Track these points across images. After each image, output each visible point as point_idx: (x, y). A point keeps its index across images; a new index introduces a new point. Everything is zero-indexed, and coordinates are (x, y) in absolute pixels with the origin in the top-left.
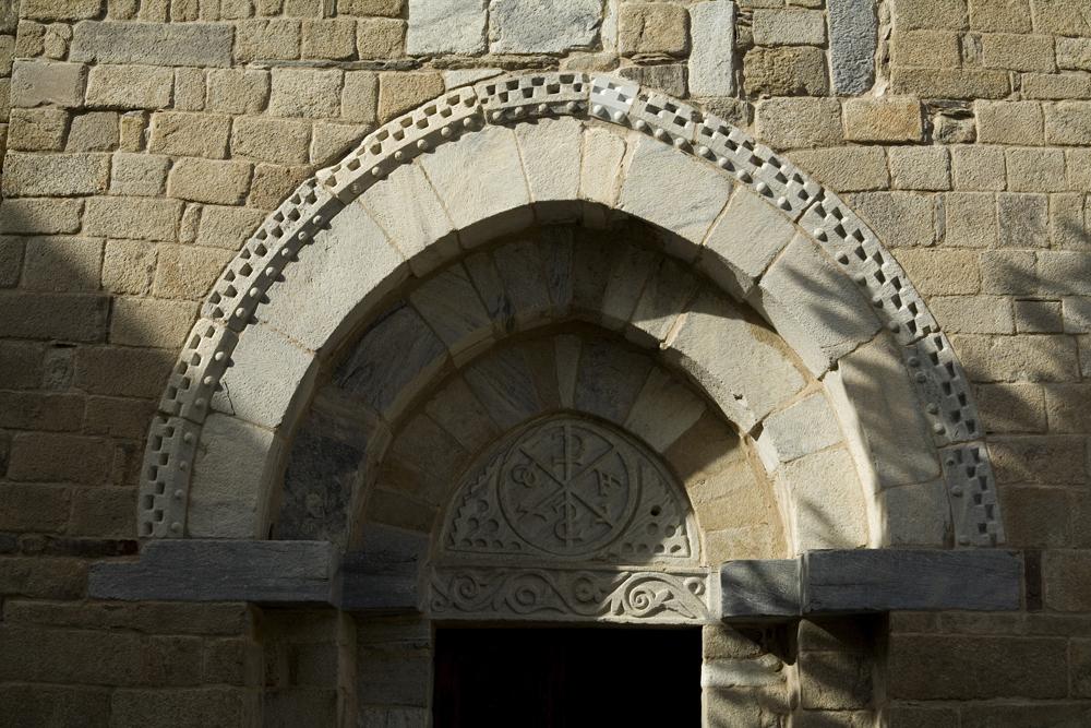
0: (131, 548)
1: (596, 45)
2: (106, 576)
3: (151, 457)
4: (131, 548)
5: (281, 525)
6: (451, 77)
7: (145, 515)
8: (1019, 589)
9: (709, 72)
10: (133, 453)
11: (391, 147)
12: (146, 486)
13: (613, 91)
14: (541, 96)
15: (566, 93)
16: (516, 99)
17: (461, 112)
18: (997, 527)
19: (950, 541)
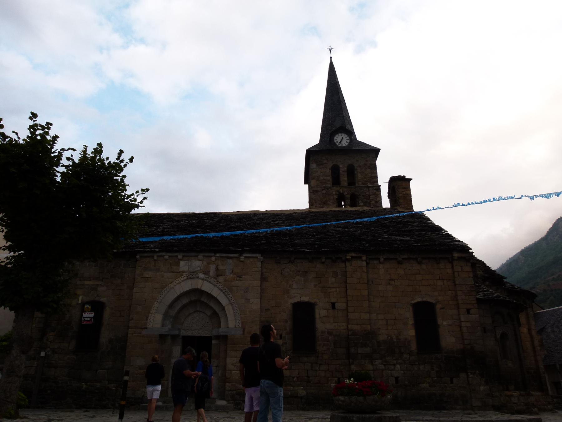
0: (146, 328)
1: (201, 269)
2: (144, 332)
3: (149, 318)
4: (146, 328)
5: (163, 326)
6: (184, 274)
7: (148, 324)
8: (242, 332)
9: (212, 273)
10: (147, 318)
11: (177, 282)
12: (149, 321)
13: (201, 275)
14: (194, 276)
15: (197, 276)
16: (191, 276)
17: (185, 278)
18: (240, 325)
19: (235, 327)
